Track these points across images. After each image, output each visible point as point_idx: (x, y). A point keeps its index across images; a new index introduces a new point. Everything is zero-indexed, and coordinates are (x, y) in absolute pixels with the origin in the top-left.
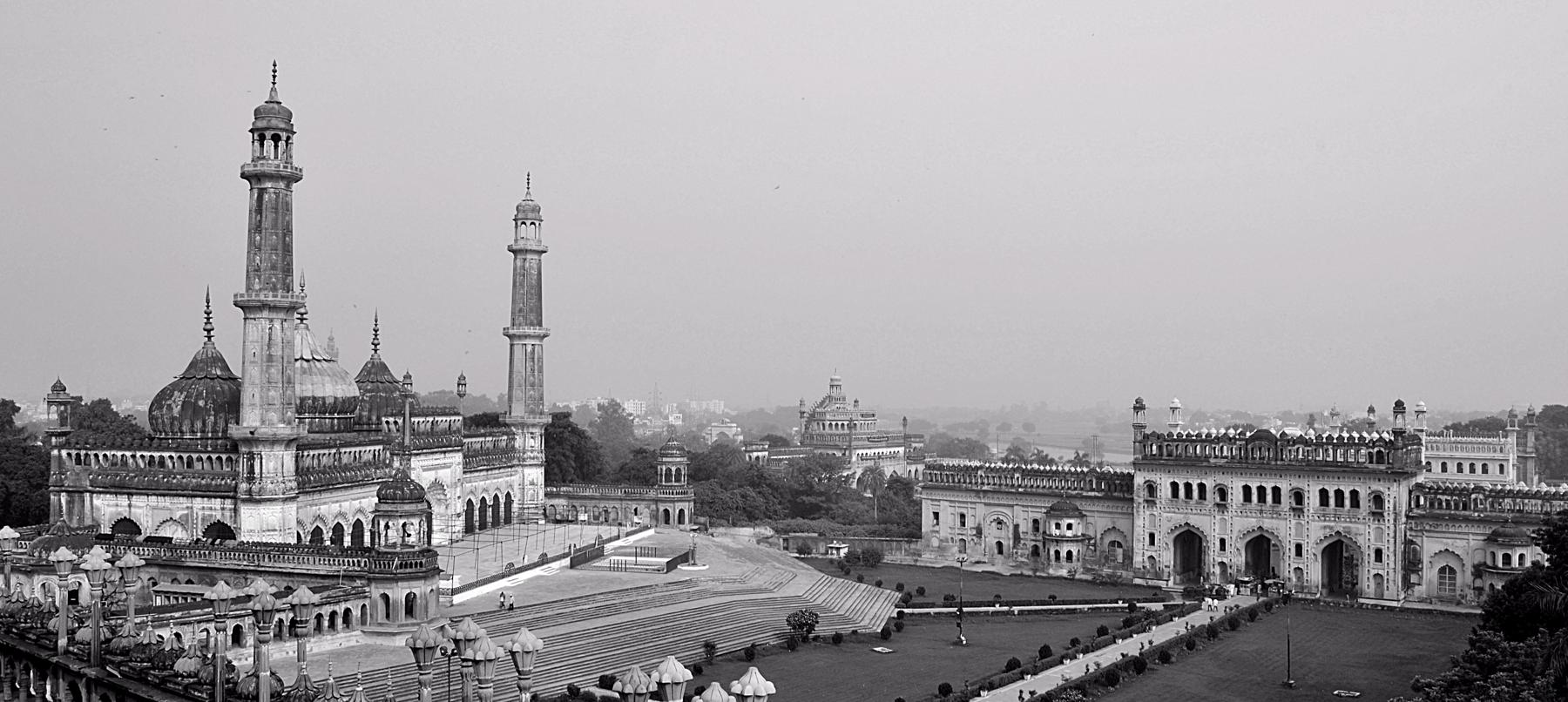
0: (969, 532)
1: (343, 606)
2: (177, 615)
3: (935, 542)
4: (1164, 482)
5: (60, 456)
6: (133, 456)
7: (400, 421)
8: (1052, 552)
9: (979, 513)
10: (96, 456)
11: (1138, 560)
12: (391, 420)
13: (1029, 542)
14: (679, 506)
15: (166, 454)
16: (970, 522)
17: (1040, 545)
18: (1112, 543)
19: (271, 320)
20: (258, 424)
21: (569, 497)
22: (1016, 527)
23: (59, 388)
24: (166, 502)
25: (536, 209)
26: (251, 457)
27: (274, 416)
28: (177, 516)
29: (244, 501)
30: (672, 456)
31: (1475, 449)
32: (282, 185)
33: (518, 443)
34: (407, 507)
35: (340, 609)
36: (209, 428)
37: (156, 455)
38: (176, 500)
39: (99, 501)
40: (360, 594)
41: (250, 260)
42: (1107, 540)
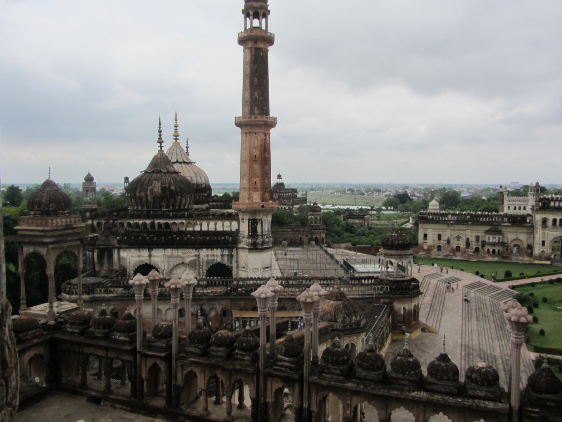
0: (443, 243)
3: (425, 247)
4: (550, 217)
5: (93, 224)
8: (491, 250)
9: (447, 233)
10: (122, 225)
11: (537, 251)
13: (474, 245)
15: (178, 221)
16: (444, 238)
17: (480, 247)
18: (515, 246)
19: (265, 134)
20: (260, 201)
22: (468, 240)
23: (89, 179)
24: (179, 252)
27: (267, 195)
28: (188, 260)
29: (250, 250)
31: (518, 202)
36: (177, 204)
38: (187, 251)
39: (124, 254)
41: (252, 95)
42: (512, 245)
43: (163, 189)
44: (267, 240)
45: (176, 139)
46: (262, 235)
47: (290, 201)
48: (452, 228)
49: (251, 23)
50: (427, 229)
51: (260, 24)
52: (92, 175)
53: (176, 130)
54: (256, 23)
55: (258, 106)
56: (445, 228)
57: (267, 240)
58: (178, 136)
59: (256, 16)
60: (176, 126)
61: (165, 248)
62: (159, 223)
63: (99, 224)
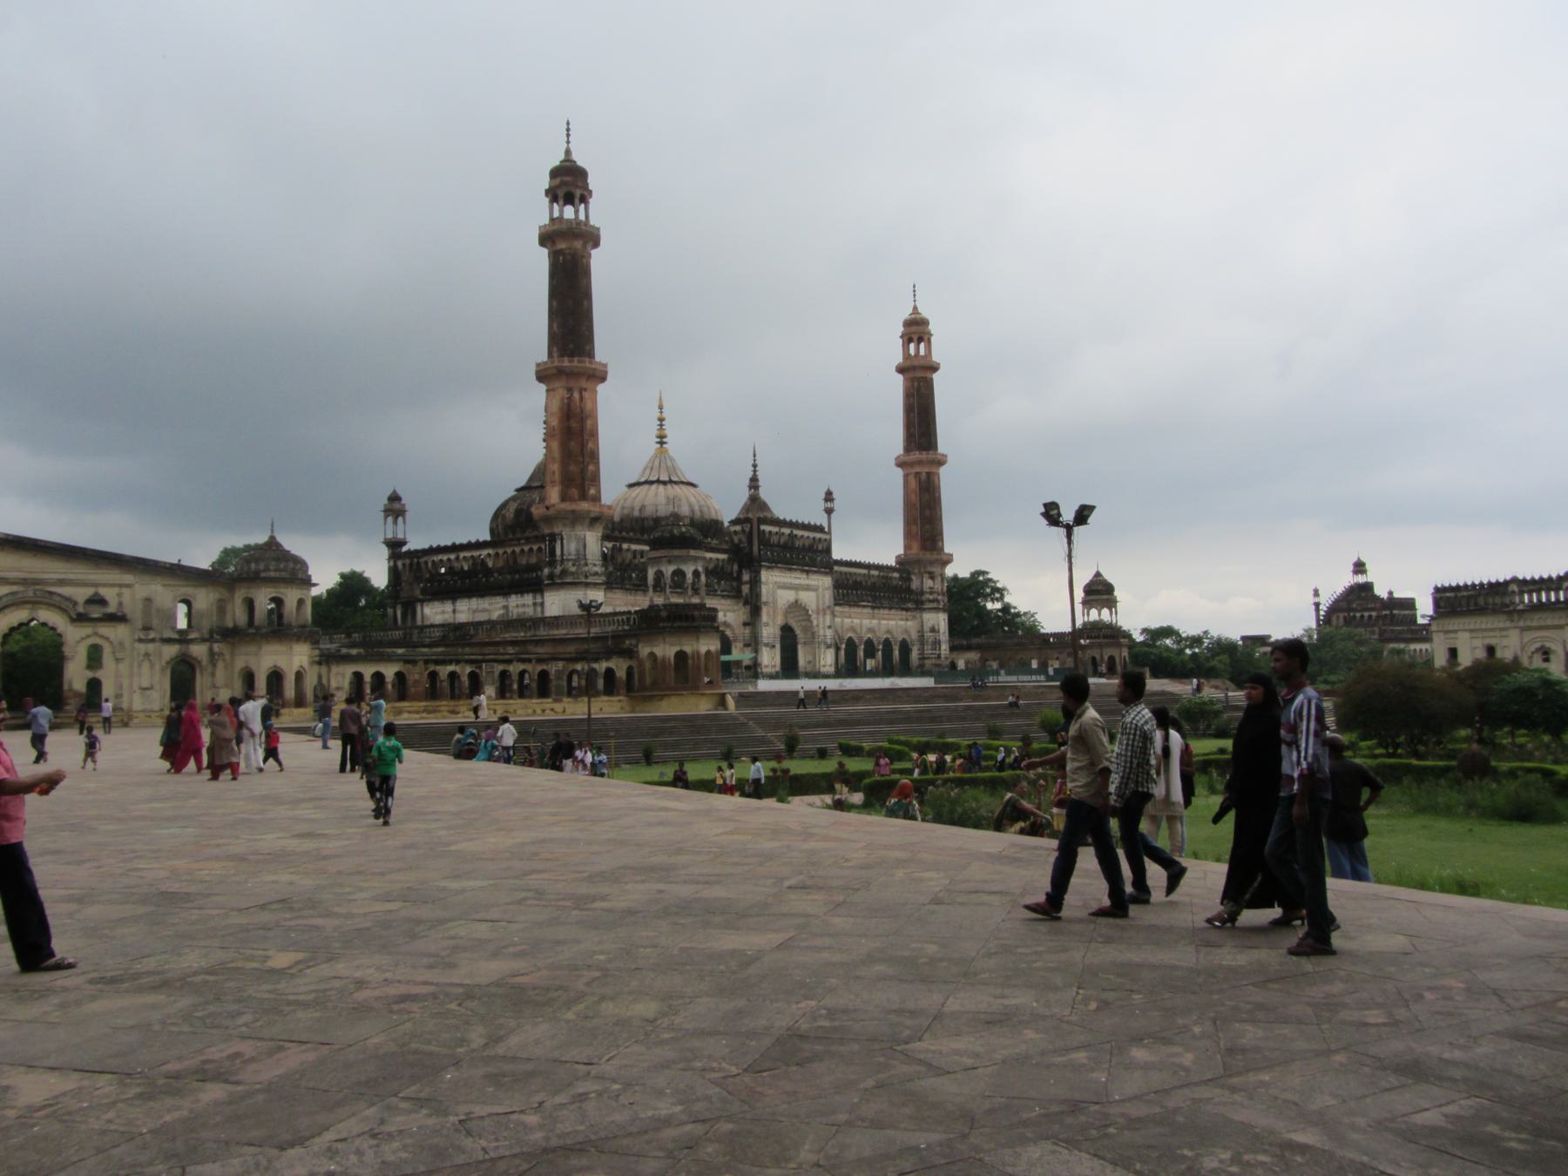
2: (400, 651)
12: (738, 528)
14: (1107, 653)
19: (570, 390)
21: (978, 648)
25: (923, 323)
26: (553, 538)
27: (574, 492)
30: (1097, 592)
32: (578, 244)
33: (915, 584)
34: (676, 552)
35: (601, 666)
37: (476, 554)
40: (630, 653)
43: (518, 512)
45: (662, 443)
46: (562, 561)
47: (1373, 633)
48: (1521, 624)
49: (561, 212)
50: (1455, 631)
51: (577, 212)
52: (400, 493)
54: (569, 212)
56: (1501, 625)
59: (569, 199)
60: (661, 420)
61: (470, 597)
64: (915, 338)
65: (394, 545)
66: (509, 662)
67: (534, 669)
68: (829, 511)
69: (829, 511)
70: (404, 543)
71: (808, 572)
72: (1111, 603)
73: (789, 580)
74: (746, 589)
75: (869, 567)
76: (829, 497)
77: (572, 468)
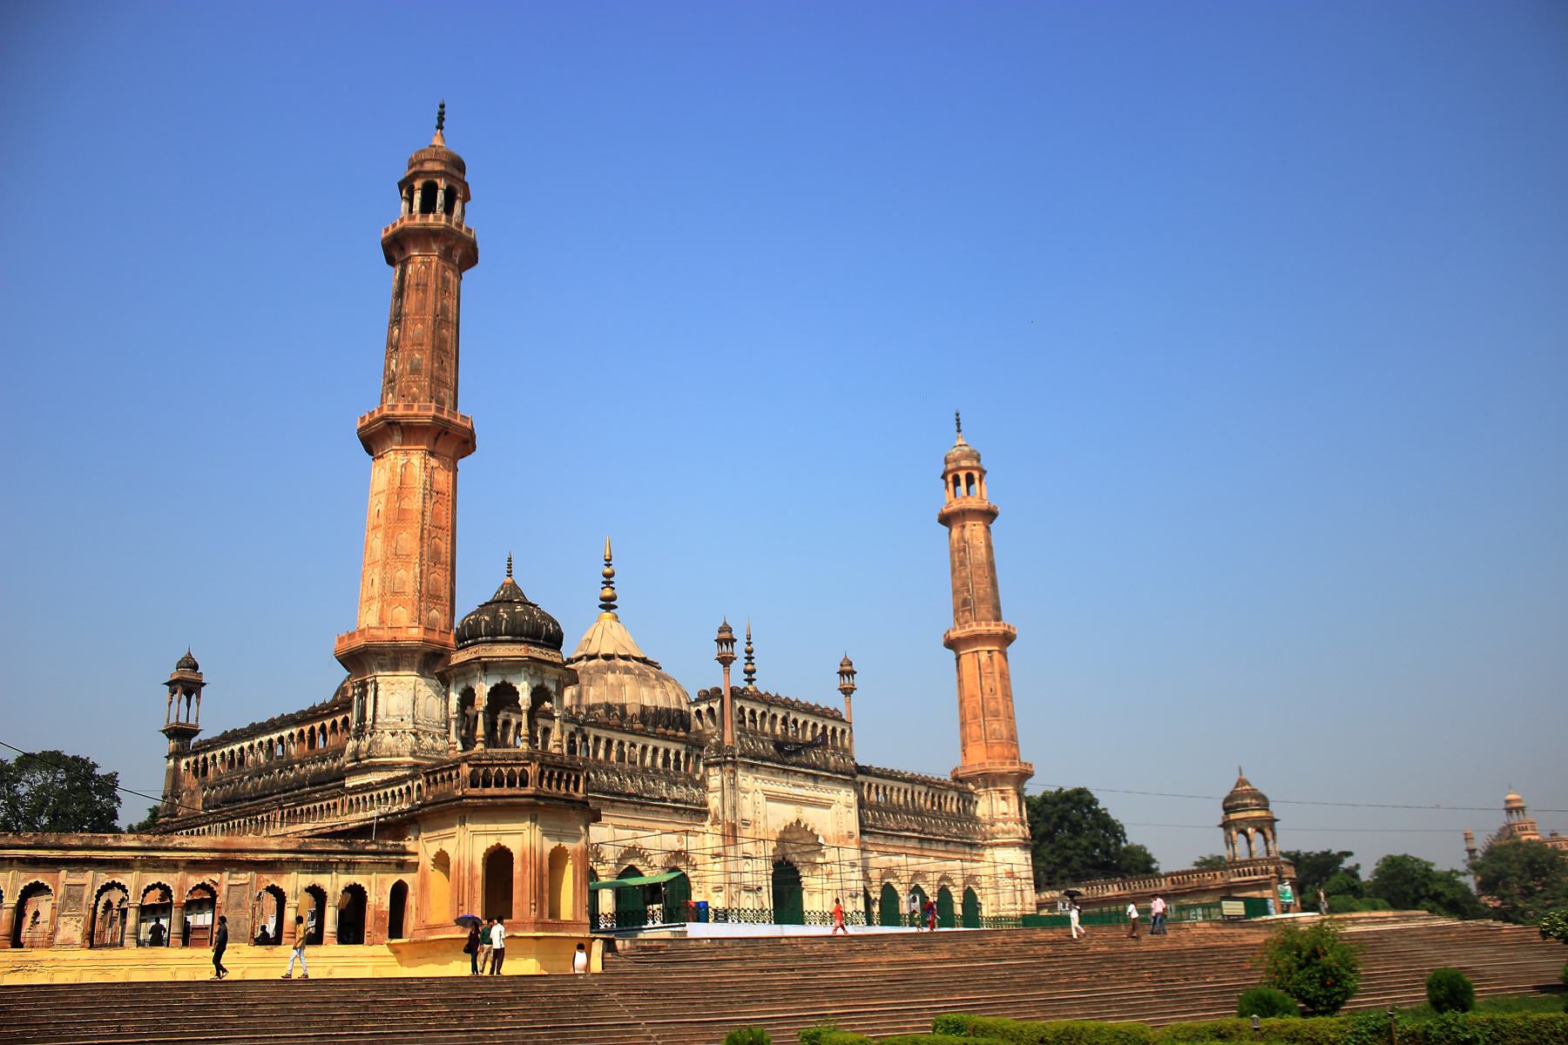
1: (345, 879)
6: (251, 747)
7: (716, 706)
30: (1245, 808)
33: (982, 809)
35: (334, 884)
44: (388, 740)
53: (608, 584)
55: (393, 389)
57: (388, 740)
58: (613, 598)
62: (261, 743)
63: (188, 764)
64: (962, 475)
65: (181, 734)
66: (125, 865)
67: (181, 883)
68: (847, 692)
69: (847, 692)
70: (196, 733)
71: (815, 778)
72: (1266, 826)
73: (787, 789)
74: (714, 801)
75: (912, 780)
76: (847, 672)
77: (401, 574)
